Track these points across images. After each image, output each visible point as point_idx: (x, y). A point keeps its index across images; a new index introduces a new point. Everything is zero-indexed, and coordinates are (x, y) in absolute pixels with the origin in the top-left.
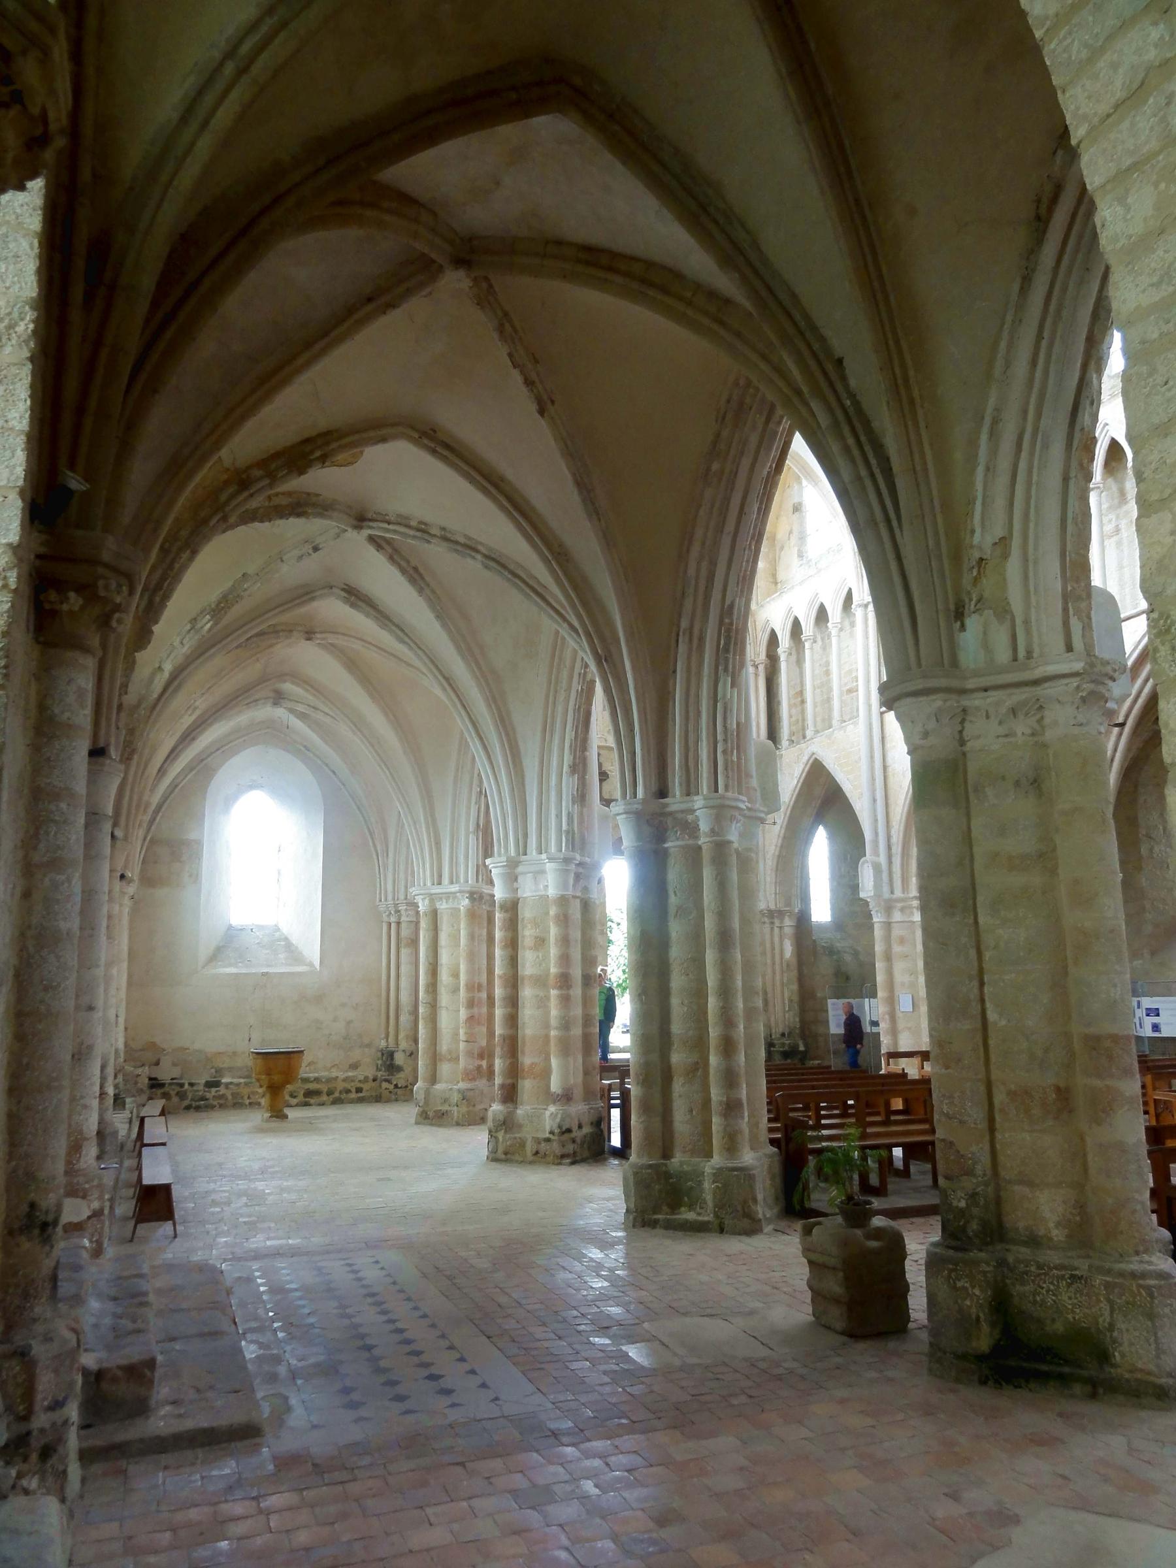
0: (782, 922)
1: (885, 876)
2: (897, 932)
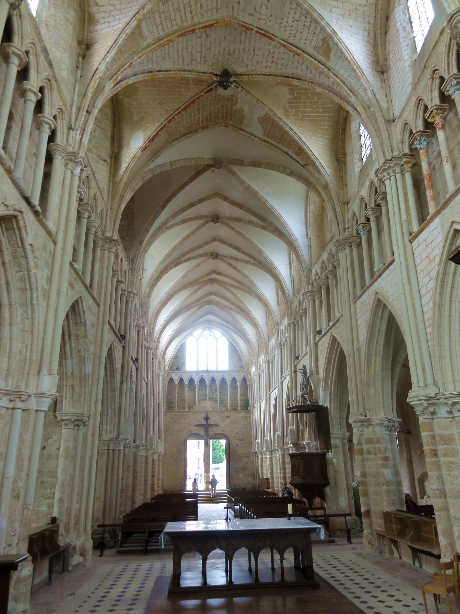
1: (260, 446)
2: (264, 460)
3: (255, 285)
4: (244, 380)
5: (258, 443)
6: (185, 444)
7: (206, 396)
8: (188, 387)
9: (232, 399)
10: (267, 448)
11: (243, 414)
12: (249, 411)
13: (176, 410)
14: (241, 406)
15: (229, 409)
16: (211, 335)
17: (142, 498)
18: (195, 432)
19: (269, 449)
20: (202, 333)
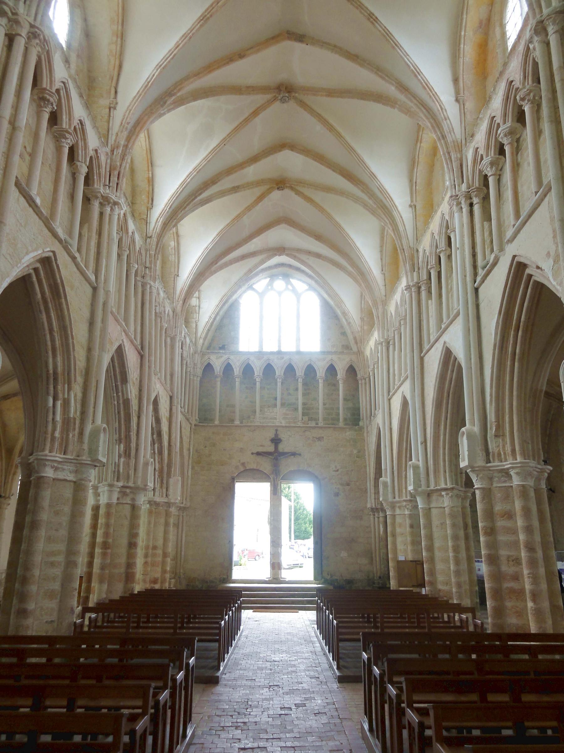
0: (379, 515)
1: (390, 489)
2: (398, 520)
3: (396, 45)
4: (352, 371)
5: (385, 484)
6: (230, 490)
7: (276, 399)
8: (241, 383)
9: (327, 406)
10: (417, 484)
11: (349, 434)
12: (361, 429)
13: (217, 422)
14: (345, 420)
15: (321, 423)
16: (287, 288)
17: (53, 604)
18: (254, 466)
19: (424, 487)
20: (270, 284)
